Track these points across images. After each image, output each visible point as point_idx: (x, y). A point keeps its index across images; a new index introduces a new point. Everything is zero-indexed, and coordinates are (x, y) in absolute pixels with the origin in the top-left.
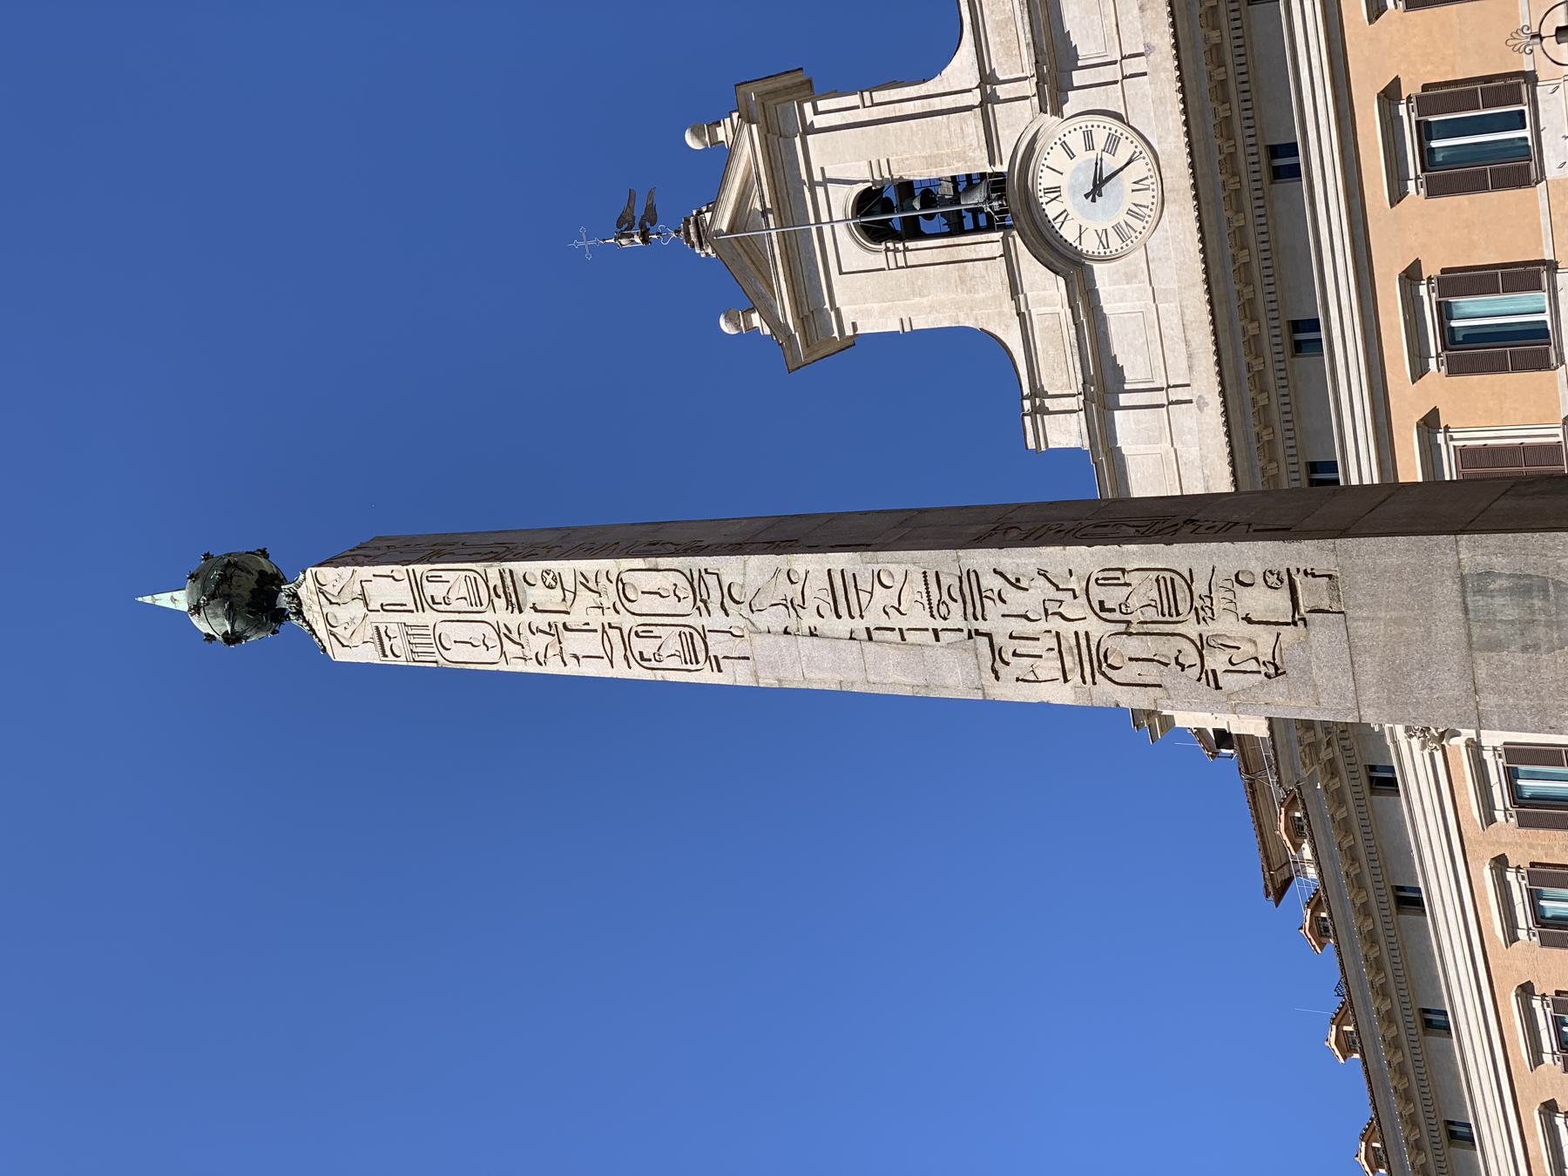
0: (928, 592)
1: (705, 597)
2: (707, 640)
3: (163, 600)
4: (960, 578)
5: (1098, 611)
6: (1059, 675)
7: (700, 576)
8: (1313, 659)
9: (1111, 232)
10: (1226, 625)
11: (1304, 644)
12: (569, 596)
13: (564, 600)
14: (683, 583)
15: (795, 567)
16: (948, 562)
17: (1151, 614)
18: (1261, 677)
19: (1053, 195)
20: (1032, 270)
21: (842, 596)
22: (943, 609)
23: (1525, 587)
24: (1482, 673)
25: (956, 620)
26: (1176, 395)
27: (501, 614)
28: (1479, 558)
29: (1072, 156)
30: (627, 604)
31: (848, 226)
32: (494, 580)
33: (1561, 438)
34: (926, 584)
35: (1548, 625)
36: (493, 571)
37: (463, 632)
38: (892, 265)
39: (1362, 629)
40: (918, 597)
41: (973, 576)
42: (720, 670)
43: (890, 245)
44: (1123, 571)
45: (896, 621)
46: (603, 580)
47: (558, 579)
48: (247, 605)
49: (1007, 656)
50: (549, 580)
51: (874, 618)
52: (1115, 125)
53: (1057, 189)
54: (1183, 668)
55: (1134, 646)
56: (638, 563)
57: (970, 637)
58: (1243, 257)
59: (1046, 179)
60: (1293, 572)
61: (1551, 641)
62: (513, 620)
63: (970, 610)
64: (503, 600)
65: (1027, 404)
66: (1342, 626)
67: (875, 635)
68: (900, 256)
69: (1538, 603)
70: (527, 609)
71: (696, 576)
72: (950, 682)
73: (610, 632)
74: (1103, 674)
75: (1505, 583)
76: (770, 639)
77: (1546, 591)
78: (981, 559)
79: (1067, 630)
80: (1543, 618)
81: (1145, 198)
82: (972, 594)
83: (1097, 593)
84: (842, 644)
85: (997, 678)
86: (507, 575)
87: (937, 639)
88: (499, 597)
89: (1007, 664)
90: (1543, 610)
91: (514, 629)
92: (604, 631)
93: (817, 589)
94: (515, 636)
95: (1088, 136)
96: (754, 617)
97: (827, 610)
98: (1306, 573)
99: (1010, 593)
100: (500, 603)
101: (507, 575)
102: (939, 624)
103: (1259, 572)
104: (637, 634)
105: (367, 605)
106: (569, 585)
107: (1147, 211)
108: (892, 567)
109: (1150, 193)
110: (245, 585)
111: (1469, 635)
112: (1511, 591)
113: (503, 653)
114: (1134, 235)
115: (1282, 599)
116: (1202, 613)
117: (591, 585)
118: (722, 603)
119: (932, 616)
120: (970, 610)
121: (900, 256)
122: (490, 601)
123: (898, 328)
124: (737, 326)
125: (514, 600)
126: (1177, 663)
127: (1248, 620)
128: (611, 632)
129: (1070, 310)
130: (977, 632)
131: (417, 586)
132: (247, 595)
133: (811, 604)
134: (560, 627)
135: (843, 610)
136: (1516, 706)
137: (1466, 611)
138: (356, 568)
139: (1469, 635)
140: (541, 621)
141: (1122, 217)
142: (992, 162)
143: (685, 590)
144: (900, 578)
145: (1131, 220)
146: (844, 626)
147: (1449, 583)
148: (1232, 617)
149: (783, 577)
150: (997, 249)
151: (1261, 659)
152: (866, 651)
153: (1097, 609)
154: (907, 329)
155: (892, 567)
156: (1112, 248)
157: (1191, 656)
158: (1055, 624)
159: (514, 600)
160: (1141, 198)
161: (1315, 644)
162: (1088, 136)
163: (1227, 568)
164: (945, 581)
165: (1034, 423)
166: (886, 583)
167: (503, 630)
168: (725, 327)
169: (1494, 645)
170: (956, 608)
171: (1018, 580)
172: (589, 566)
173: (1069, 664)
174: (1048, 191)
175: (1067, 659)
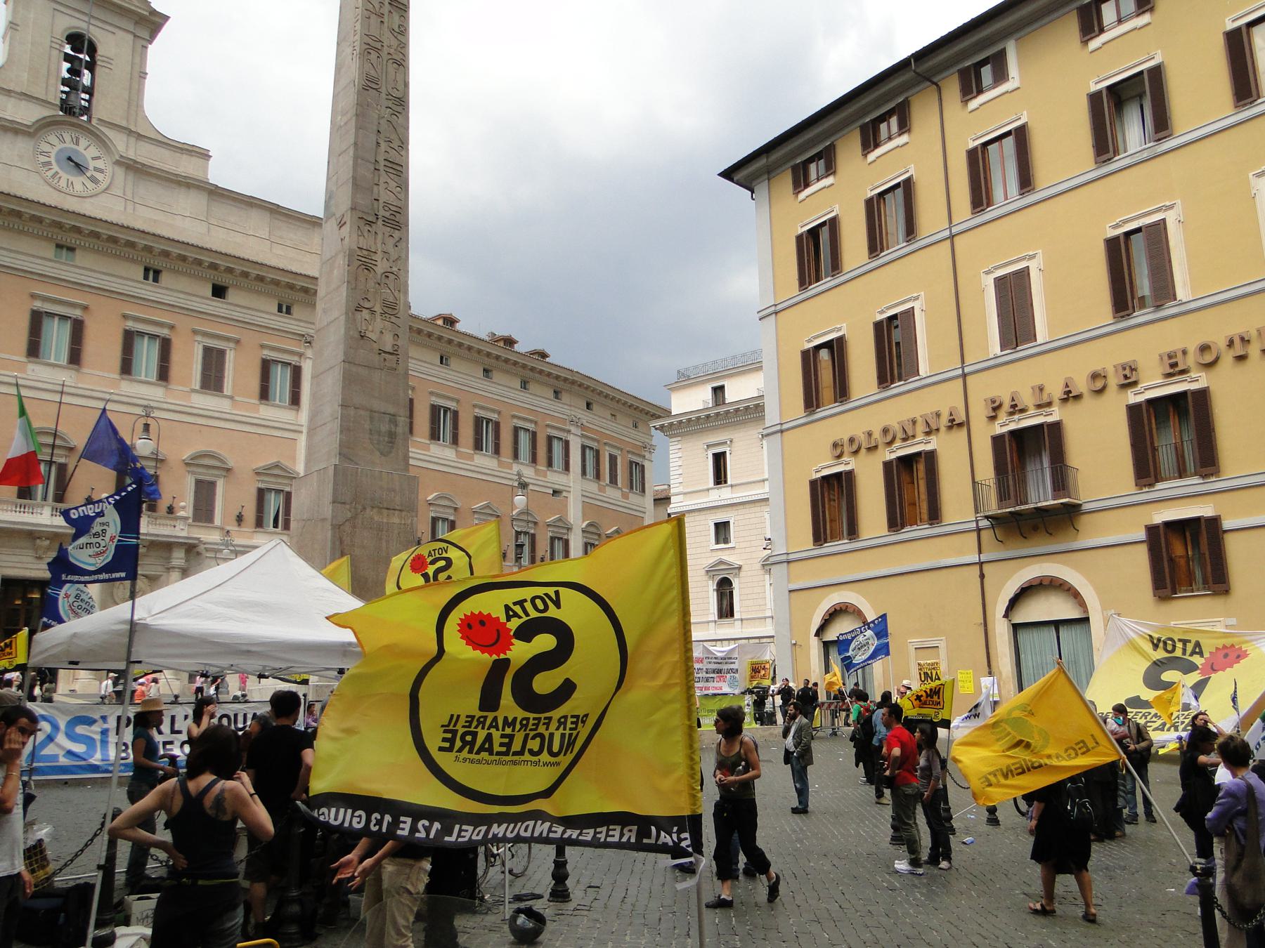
2: (374, 91)
7: (401, 105)
9: (47, 159)
12: (396, 34)
24: (362, 413)
45: (382, 186)
46: (401, 56)
51: (384, 178)
52: (103, 186)
53: (77, 144)
55: (371, 284)
59: (84, 142)
75: (393, 430)
77: (391, 442)
81: (63, 183)
83: (392, 277)
93: (393, 155)
99: (391, 242)
102: (381, 201)
106: (399, 37)
107: (55, 181)
109: (65, 186)
111: (375, 412)
115: (388, 348)
133: (389, 149)
137: (384, 413)
139: (375, 412)
146: (382, 163)
148: (382, 326)
157: (367, 305)
160: (63, 183)
162: (101, 171)
164: (397, 215)
169: (372, 418)
170: (387, 214)
174: (77, 139)
175: (365, 253)
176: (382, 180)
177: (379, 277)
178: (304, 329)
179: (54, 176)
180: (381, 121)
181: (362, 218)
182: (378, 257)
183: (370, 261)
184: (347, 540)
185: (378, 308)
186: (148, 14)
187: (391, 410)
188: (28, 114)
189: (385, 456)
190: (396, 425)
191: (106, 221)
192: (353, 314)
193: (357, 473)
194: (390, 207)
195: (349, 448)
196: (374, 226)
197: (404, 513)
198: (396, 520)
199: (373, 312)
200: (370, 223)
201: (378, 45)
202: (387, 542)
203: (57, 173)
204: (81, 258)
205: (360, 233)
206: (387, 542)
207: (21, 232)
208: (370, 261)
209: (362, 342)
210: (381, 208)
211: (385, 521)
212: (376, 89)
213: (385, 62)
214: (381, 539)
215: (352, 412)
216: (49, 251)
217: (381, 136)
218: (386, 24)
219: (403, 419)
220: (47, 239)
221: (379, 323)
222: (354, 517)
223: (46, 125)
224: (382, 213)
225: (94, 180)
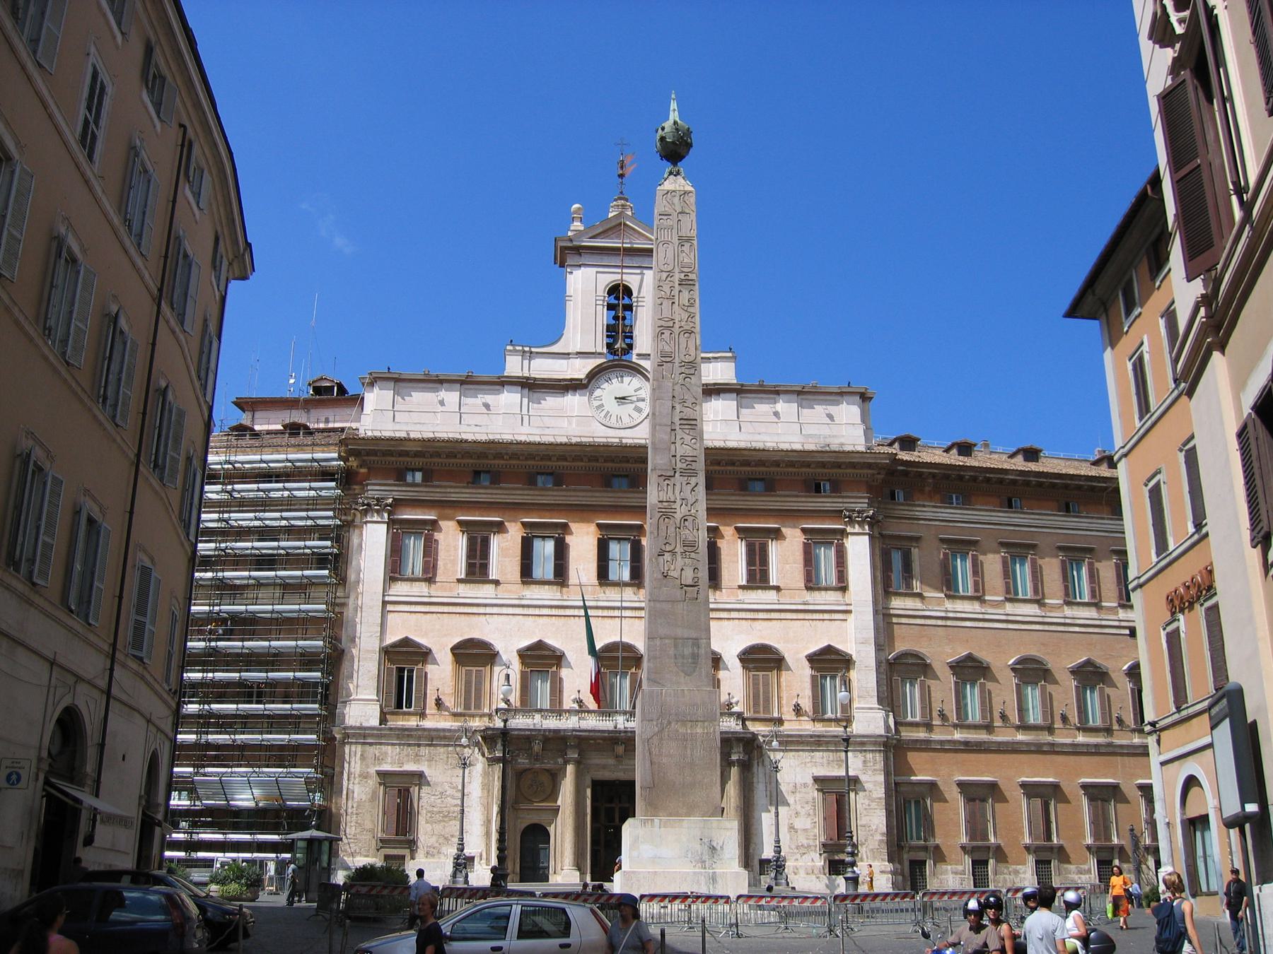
3: (673, 105)
6: (661, 499)
9: (600, 403)
10: (680, 562)
12: (686, 308)
17: (684, 536)
20: (592, 364)
22: (683, 461)
24: (667, 641)
25: (679, 465)
26: (526, 418)
27: (677, 276)
32: (692, 276)
33: (490, 578)
35: (683, 663)
37: (670, 254)
38: (598, 298)
39: (680, 606)
45: (679, 442)
46: (692, 325)
47: (692, 305)
49: (667, 482)
50: (692, 301)
55: (672, 529)
56: (698, 342)
58: (585, 459)
64: (683, 278)
65: (527, 349)
67: (673, 433)
68: (601, 302)
70: (680, 288)
73: (672, 322)
77: (694, 663)
79: (677, 505)
81: (614, 419)
83: (690, 519)
93: (688, 413)
94: (669, 279)
97: (682, 415)
99: (689, 487)
100: (682, 276)
102: (678, 458)
105: (680, 213)
106: (691, 309)
113: (662, 271)
115: (690, 582)
121: (601, 302)
122: (683, 272)
123: (567, 294)
124: (575, 212)
127: (682, 569)
128: (672, 322)
133: (684, 409)
140: (676, 292)
141: (606, 408)
144: (695, 446)
145: (604, 413)
149: (694, 400)
150: (599, 350)
154: (567, 298)
157: (668, 548)
160: (614, 419)
168: (576, 206)
169: (676, 646)
170: (684, 466)
175: (666, 504)
176: (678, 438)
178: (841, 505)
179: (605, 417)
180: (676, 387)
181: (662, 475)
182: (677, 505)
185: (679, 549)
187: (694, 635)
188: (579, 369)
192: (656, 559)
193: (662, 693)
194: (686, 458)
196: (672, 479)
197: (706, 724)
198: (699, 730)
199: (673, 552)
201: (671, 324)
202: (692, 750)
203: (608, 412)
206: (692, 750)
210: (678, 461)
211: (689, 731)
213: (677, 337)
214: (686, 747)
215: (658, 642)
218: (677, 303)
221: (680, 562)
222: (661, 731)
223: (595, 375)
224: (679, 465)
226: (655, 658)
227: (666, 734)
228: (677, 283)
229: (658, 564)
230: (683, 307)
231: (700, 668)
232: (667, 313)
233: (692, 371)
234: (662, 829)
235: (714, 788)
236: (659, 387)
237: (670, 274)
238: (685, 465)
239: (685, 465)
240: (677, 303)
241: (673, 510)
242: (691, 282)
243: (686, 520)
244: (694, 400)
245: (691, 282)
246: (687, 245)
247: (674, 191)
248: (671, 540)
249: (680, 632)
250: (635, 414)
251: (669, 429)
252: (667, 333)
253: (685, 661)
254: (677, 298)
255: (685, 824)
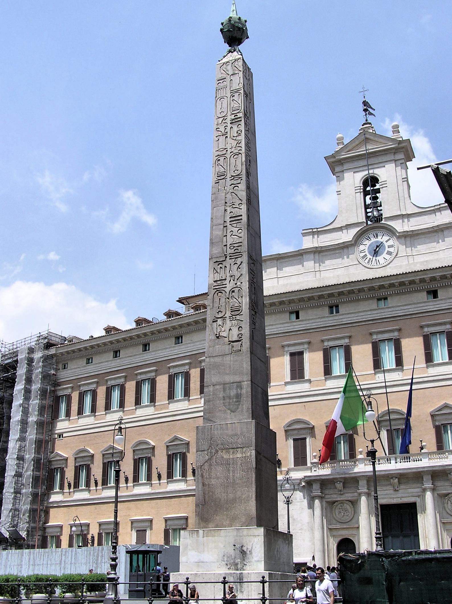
0: (236, 243)
1: (235, 179)
4: (240, 252)
5: (232, 290)
7: (240, 178)
8: (220, 346)
9: (364, 254)
10: (228, 323)
11: (224, 344)
12: (235, 138)
13: (234, 137)
14: (238, 172)
15: (243, 205)
16: (245, 248)
18: (216, 333)
19: (375, 236)
21: (236, 219)
22: (232, 247)
23: (238, 396)
24: (218, 387)
25: (229, 251)
27: (230, 118)
28: (245, 386)
29: (386, 242)
30: (233, 156)
31: (367, 175)
33: (306, 378)
34: (239, 243)
35: (229, 402)
36: (241, 115)
37: (225, 105)
38: (356, 188)
39: (228, 358)
40: (235, 240)
41: (241, 256)
42: (215, 183)
43: (362, 187)
44: (242, 297)
45: (229, 234)
46: (239, 148)
47: (239, 135)
48: (232, 36)
49: (220, 266)
50: (239, 132)
52: (395, 254)
54: (218, 313)
55: (223, 300)
56: (244, 159)
57: (225, 255)
60: (242, 341)
61: (226, 403)
62: (228, 121)
63: (232, 255)
66: (228, 353)
69: (235, 400)
70: (231, 125)
71: (240, 176)
72: (214, 249)
73: (225, 150)
74: (216, 292)
75: (239, 392)
76: (224, 198)
77: (237, 402)
78: (245, 258)
79: (227, 282)
80: (231, 401)
82: (237, 255)
83: (236, 290)
84: (223, 219)
85: (214, 262)
86: (240, 119)
87: (224, 246)
88: (235, 116)
89: (218, 265)
90: (233, 401)
91: (226, 121)
92: (225, 149)
93: (236, 212)
94: (224, 121)
95: (391, 246)
96: (229, 193)
98: (241, 344)
99: (236, 266)
101: (240, 119)
102: (228, 246)
103: (242, 332)
104: (225, 159)
105: (232, 75)
106: (238, 138)
107: (370, 264)
108: (243, 233)
109: (375, 264)
110: (237, 35)
111: (227, 384)
112: (237, 394)
114: (364, 260)
115: (235, 338)
116: (231, 318)
117: (238, 144)
118: (233, 184)
119: (230, 244)
120: (232, 255)
125: (233, 121)
126: (219, 311)
127: (230, 329)
129: (342, 242)
130: (226, 257)
131: (237, 91)
132: (234, 35)
133: (233, 210)
134: (226, 136)
135: (232, 219)
136: (210, 395)
137: (233, 383)
138: (242, 72)
139: (227, 384)
140: (228, 129)
142: (385, 218)
143: (237, 173)
145: (368, 259)
146: (228, 219)
147: (239, 379)
148: (231, 325)
149: (240, 202)
151: (220, 333)
152: (221, 226)
153: (232, 290)
155: (243, 233)
156: (360, 254)
157: (220, 315)
158: (228, 279)
159: (233, 121)
161: (224, 346)
162: (391, 246)
163: (243, 324)
165: (310, 232)
166: (239, 231)
167: (225, 118)
169: (224, 390)
170: (232, 251)
171: (240, 268)
172: (243, 144)
173: (218, 282)
175: (220, 282)
176: (229, 231)
177: (228, 293)
181: (217, 262)
183: (222, 286)
184: (206, 475)
186: (397, 145)
187: (237, 379)
188: (348, 236)
189: (234, 412)
190: (241, 389)
191: (421, 271)
192: (211, 325)
193: (211, 428)
194: (235, 245)
195: (210, 413)
196: (224, 263)
197: (244, 449)
198: (239, 455)
200: (220, 263)
201: (224, 152)
202: (234, 472)
204: (391, 302)
205: (215, 272)
207: (358, 300)
208: (222, 286)
209: (217, 341)
211: (231, 457)
212: (223, 179)
213: (229, 159)
214: (229, 470)
216: (373, 304)
217: (226, 205)
218: (229, 137)
219: (246, 383)
220: (373, 298)
225: (389, 253)
226: (209, 401)
227: (214, 462)
228: (229, 122)
229: (213, 328)
230: (233, 138)
231: (243, 405)
232: (222, 146)
233: (239, 181)
234: (205, 538)
235: (250, 502)
236: (216, 198)
237: (224, 118)
238: (233, 250)
239: (233, 250)
240: (229, 137)
241: (224, 286)
242: (239, 120)
243: (233, 291)
244: (240, 202)
245: (239, 120)
246: (236, 95)
247: (228, 62)
248: (222, 309)
249: (228, 379)
250: (388, 257)
251: (222, 227)
252: (222, 159)
253: (231, 401)
254: (229, 133)
255: (223, 533)
